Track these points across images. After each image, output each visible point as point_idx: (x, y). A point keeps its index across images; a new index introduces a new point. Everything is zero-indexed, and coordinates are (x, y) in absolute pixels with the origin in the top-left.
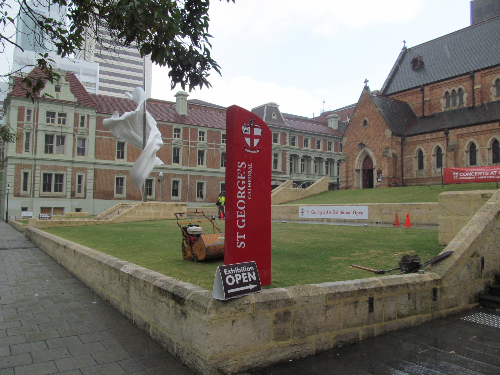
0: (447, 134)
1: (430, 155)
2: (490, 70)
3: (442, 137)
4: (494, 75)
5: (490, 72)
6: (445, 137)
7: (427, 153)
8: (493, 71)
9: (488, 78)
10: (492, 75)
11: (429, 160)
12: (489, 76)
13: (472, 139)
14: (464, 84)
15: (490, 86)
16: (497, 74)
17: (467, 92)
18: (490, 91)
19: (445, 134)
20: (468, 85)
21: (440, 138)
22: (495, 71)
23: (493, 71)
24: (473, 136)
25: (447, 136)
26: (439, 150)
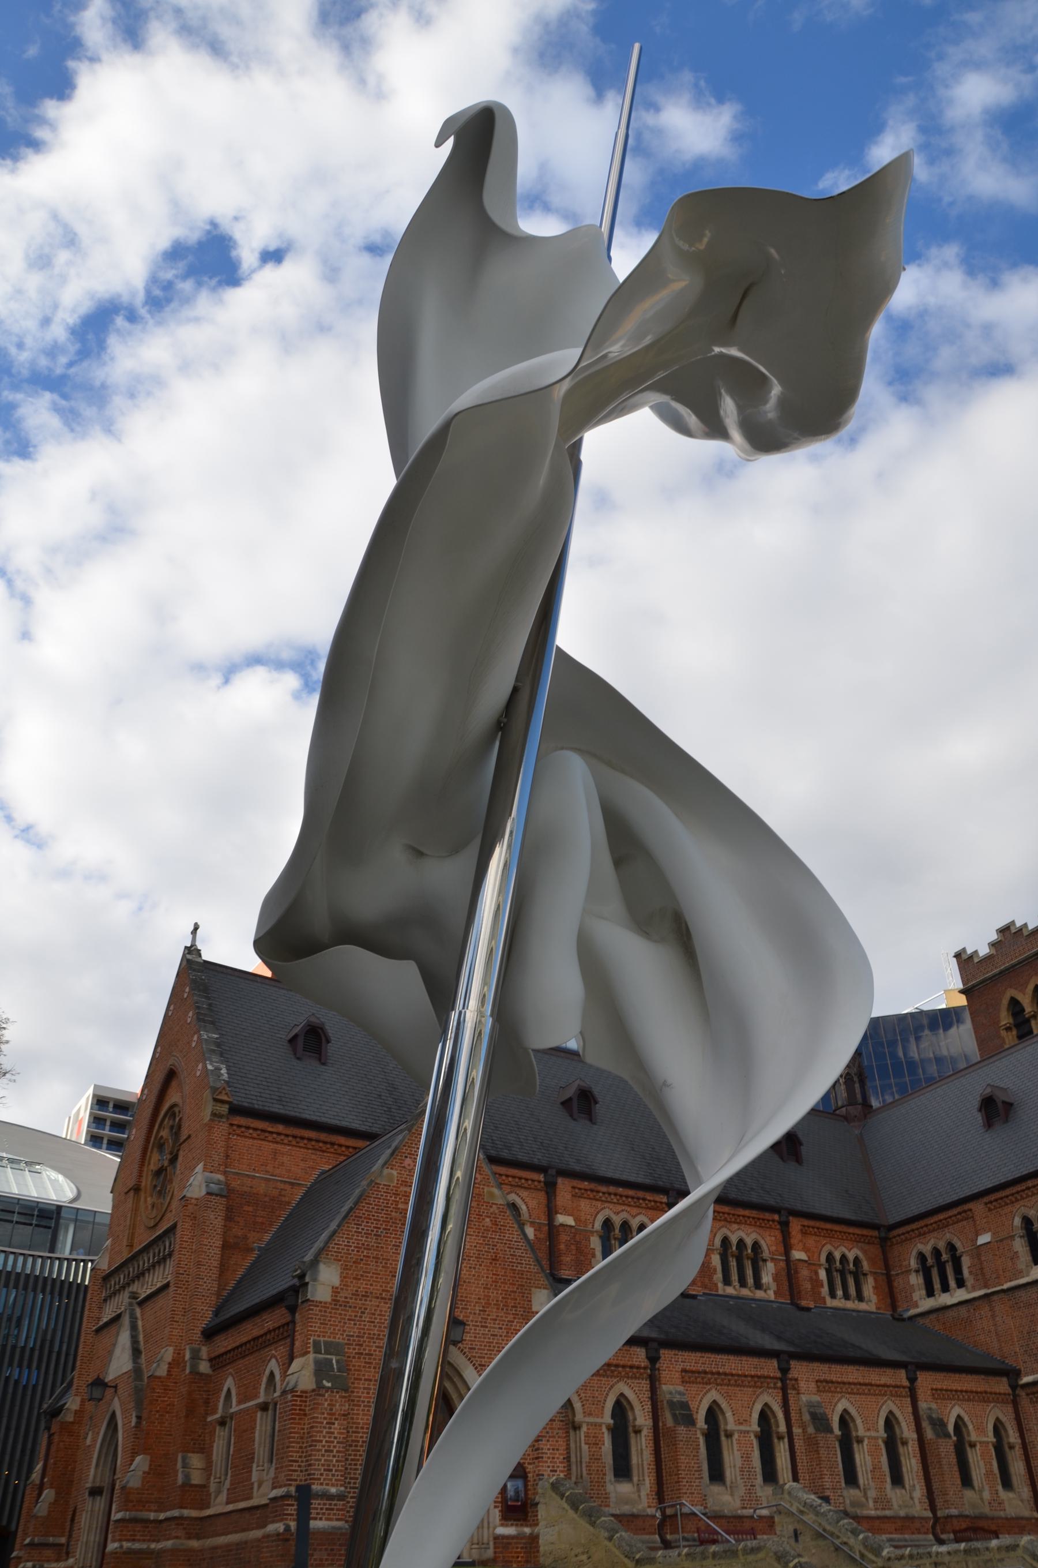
0: (653, 1359)
1: (600, 1425)
2: (593, 1186)
3: (638, 1368)
4: (599, 1204)
5: (592, 1191)
6: (645, 1368)
7: (590, 1414)
8: (598, 1192)
9: (584, 1205)
10: (594, 1202)
11: (595, 1443)
12: (588, 1201)
13: (713, 1395)
14: (524, 1194)
15: (592, 1232)
16: (606, 1205)
17: (532, 1224)
18: (592, 1246)
19: (648, 1358)
20: (535, 1202)
21: (631, 1367)
22: (604, 1193)
23: (598, 1192)
24: (717, 1385)
25: (653, 1369)
26: (621, 1408)
